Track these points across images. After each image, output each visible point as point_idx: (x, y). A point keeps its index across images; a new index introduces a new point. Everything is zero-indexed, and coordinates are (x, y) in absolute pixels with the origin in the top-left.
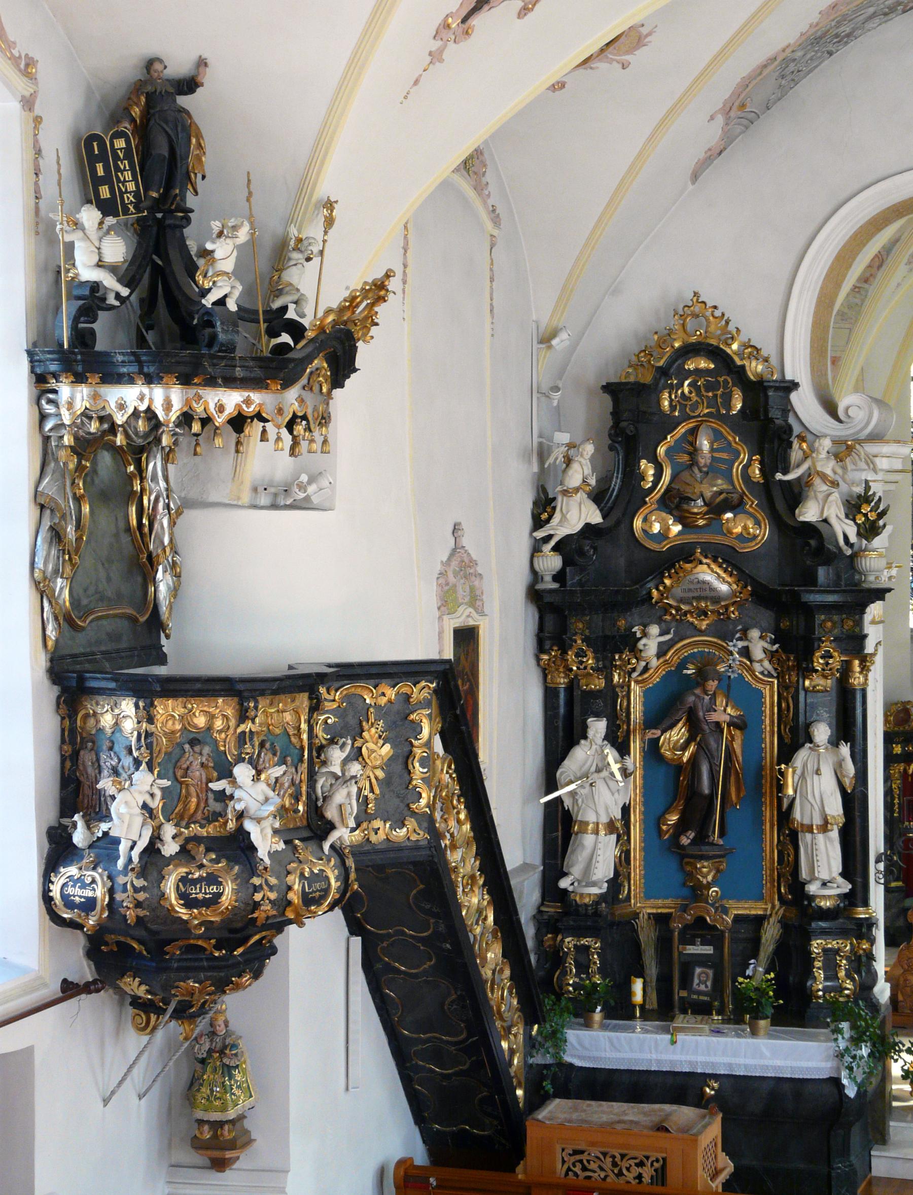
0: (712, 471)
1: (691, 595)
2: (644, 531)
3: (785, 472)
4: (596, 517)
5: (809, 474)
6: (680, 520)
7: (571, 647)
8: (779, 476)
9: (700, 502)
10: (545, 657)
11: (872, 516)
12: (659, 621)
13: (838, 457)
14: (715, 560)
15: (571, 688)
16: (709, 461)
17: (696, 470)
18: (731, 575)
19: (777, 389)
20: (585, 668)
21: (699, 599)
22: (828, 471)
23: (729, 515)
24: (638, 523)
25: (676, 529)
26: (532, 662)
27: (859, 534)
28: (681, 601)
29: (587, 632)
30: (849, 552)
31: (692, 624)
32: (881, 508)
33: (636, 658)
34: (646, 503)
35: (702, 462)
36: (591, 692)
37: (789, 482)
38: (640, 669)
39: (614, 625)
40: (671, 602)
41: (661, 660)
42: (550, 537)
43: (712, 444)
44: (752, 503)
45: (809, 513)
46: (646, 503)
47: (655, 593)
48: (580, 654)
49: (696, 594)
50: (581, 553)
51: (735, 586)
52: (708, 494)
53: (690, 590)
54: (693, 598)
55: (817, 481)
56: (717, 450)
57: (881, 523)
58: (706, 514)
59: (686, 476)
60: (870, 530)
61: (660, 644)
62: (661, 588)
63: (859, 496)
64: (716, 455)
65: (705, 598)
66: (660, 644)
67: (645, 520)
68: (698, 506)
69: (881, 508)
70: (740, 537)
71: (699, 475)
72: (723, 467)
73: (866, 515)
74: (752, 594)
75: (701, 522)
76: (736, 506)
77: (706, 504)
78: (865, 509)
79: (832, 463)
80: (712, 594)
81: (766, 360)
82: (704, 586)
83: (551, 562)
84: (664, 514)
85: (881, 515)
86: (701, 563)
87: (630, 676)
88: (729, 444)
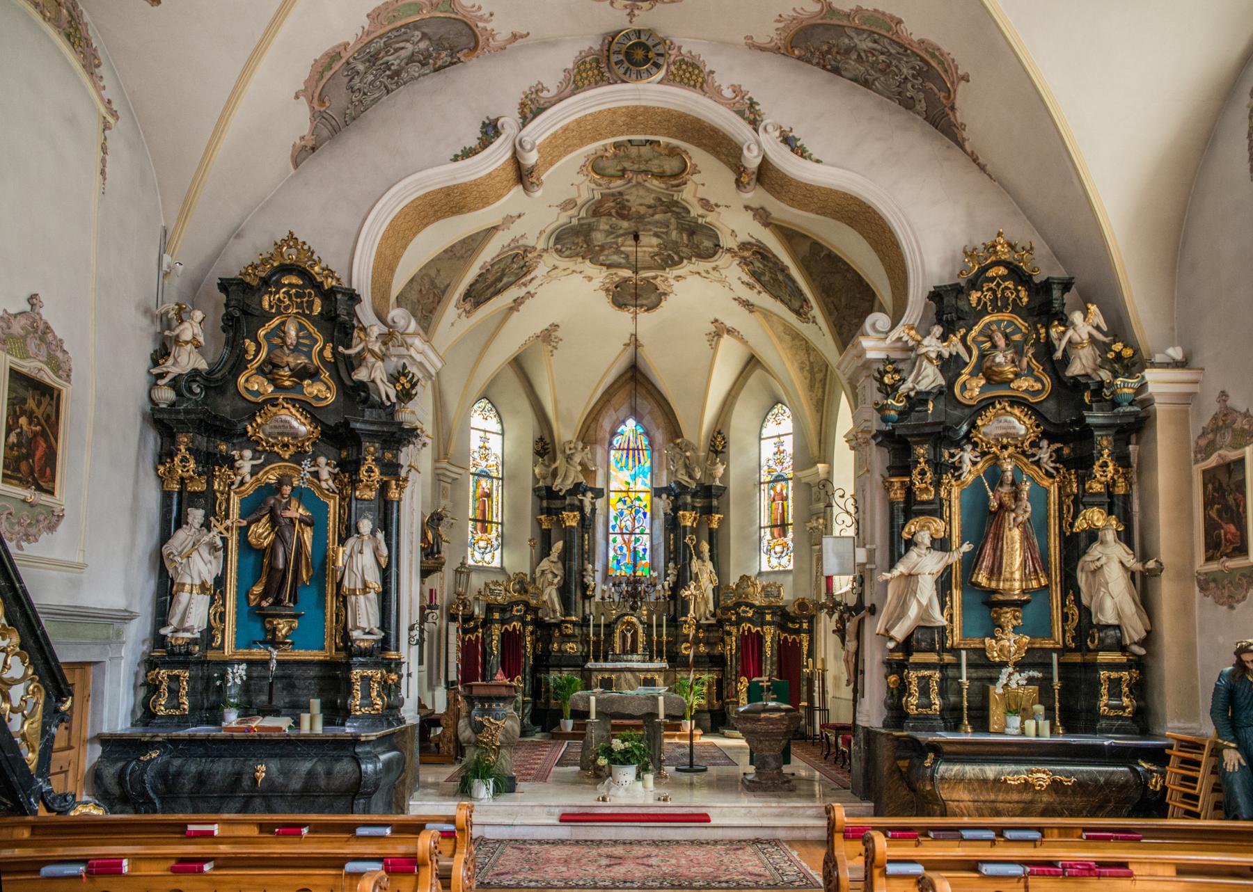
0: (296, 349)
1: (276, 431)
2: (247, 389)
3: (348, 347)
4: (203, 365)
5: (363, 349)
6: (272, 381)
7: (176, 455)
8: (341, 349)
9: (287, 369)
10: (162, 469)
11: (408, 386)
12: (255, 451)
13: (385, 343)
14: (294, 406)
15: (180, 493)
16: (295, 343)
17: (285, 348)
18: (306, 418)
19: (344, 294)
20: (188, 471)
21: (282, 434)
22: (376, 349)
23: (306, 382)
24: (242, 380)
25: (270, 389)
26: (152, 472)
27: (397, 397)
28: (269, 435)
29: (190, 445)
30: (389, 404)
31: (278, 454)
32: (415, 380)
33: (235, 475)
34: (247, 368)
35: (289, 342)
36: (195, 493)
37: (349, 356)
38: (237, 483)
39: (217, 447)
40: (261, 435)
41: (254, 478)
42: (167, 373)
43: (298, 332)
44: (325, 375)
45: (361, 375)
46: (247, 368)
47: (249, 429)
48: (184, 460)
49: (280, 430)
50: (190, 391)
51: (308, 427)
52: (292, 365)
53: (275, 427)
54: (279, 434)
55: (369, 356)
56: (303, 338)
57: (414, 392)
58: (290, 377)
59: (278, 352)
60: (406, 395)
61: (253, 466)
62: (254, 425)
63: (399, 372)
64: (301, 341)
65: (288, 435)
66: (253, 466)
67: (247, 381)
68: (286, 372)
69: (415, 380)
70: (316, 398)
71: (287, 352)
72: (305, 349)
73: (403, 385)
74: (322, 433)
75: (287, 383)
76: (314, 375)
77: (291, 370)
78: (403, 380)
79: (379, 344)
80: (292, 431)
81: (338, 280)
82: (286, 425)
83: (166, 395)
84: (261, 378)
85: (413, 386)
86: (283, 407)
87: (230, 489)
88: (310, 333)
